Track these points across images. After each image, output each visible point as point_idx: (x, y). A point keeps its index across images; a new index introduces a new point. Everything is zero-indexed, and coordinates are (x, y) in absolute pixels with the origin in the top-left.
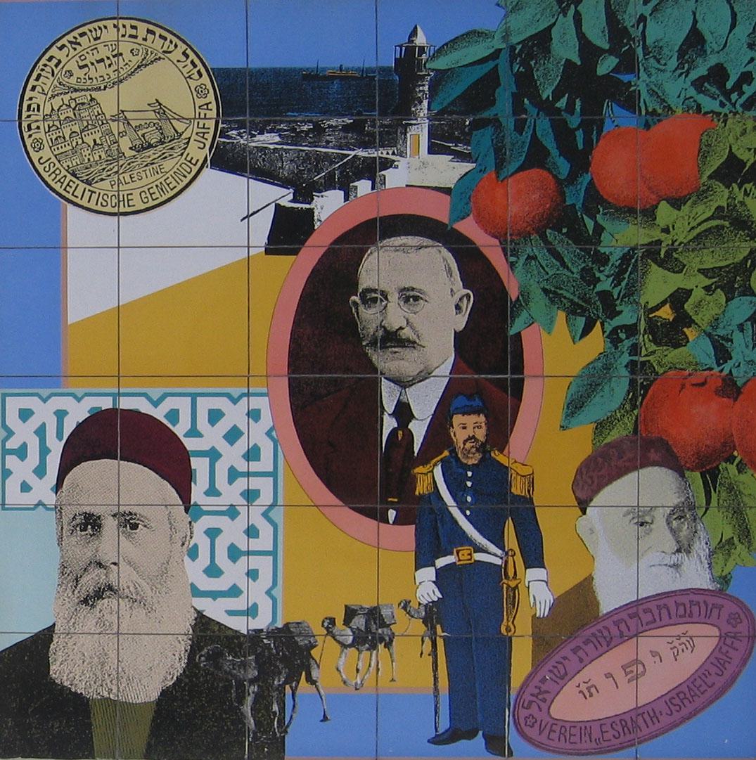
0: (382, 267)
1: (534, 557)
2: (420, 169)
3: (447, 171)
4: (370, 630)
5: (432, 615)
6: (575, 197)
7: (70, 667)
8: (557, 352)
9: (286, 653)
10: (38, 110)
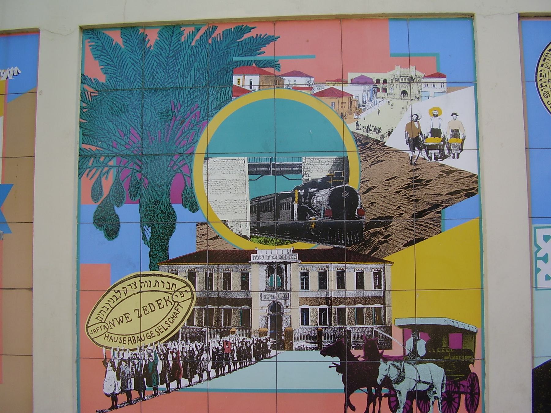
10: (546, 77)
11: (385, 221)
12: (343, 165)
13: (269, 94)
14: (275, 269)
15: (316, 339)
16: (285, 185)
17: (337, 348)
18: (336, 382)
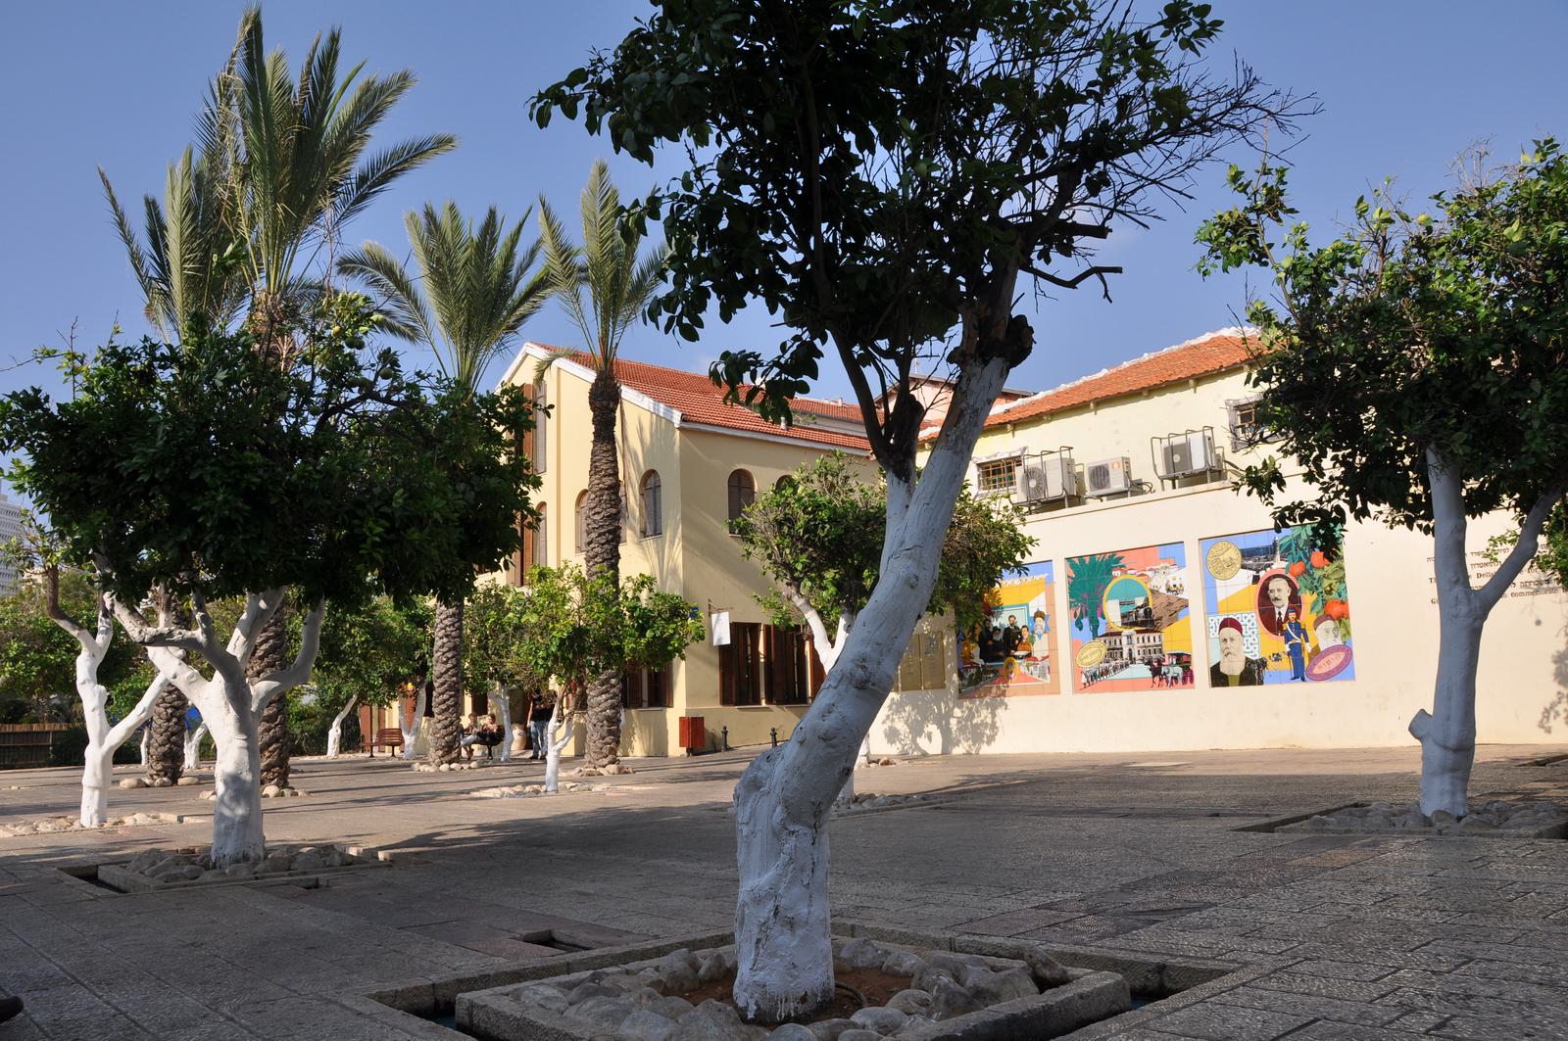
0: (1273, 585)
1: (1307, 641)
2: (1279, 565)
3: (1284, 564)
4: (1277, 658)
5: (1289, 654)
6: (1308, 567)
7: (1223, 669)
8: (1308, 598)
9: (1262, 664)
11: (1160, 618)
12: (1147, 600)
13: (1123, 577)
14: (1129, 637)
15: (1142, 660)
16: (1130, 608)
17: (1149, 663)
18: (1149, 674)
